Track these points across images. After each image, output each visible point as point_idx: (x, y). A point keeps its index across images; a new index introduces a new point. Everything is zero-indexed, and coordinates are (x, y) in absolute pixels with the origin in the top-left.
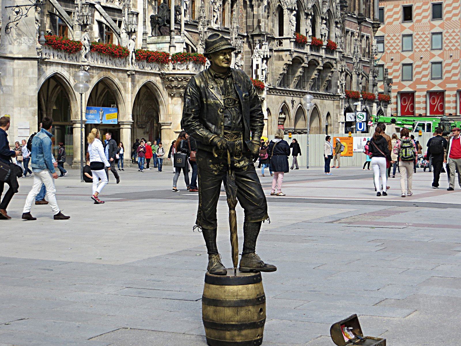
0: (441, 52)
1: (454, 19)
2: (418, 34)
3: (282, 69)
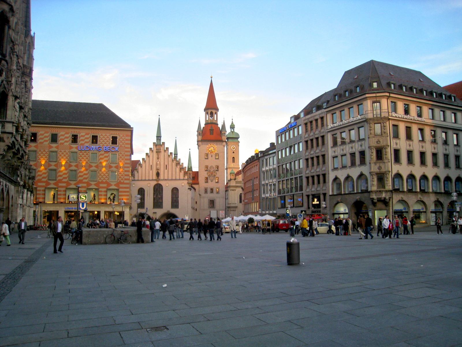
0: (56, 163)
1: (65, 144)
2: (40, 151)
3: (2, 150)
